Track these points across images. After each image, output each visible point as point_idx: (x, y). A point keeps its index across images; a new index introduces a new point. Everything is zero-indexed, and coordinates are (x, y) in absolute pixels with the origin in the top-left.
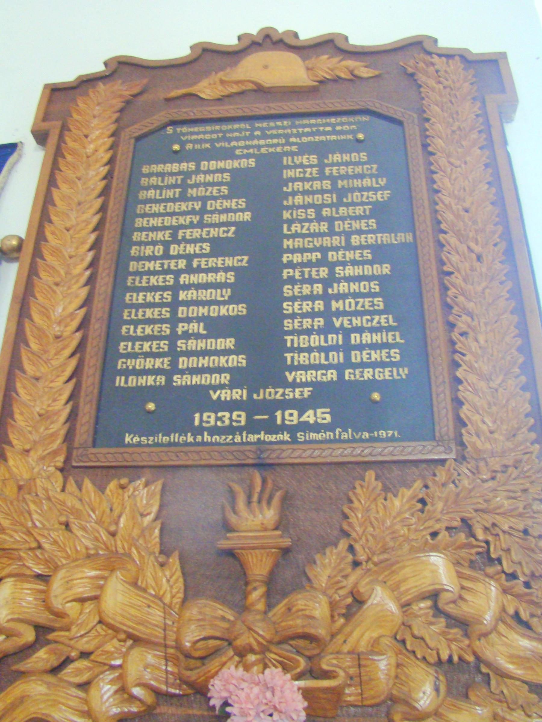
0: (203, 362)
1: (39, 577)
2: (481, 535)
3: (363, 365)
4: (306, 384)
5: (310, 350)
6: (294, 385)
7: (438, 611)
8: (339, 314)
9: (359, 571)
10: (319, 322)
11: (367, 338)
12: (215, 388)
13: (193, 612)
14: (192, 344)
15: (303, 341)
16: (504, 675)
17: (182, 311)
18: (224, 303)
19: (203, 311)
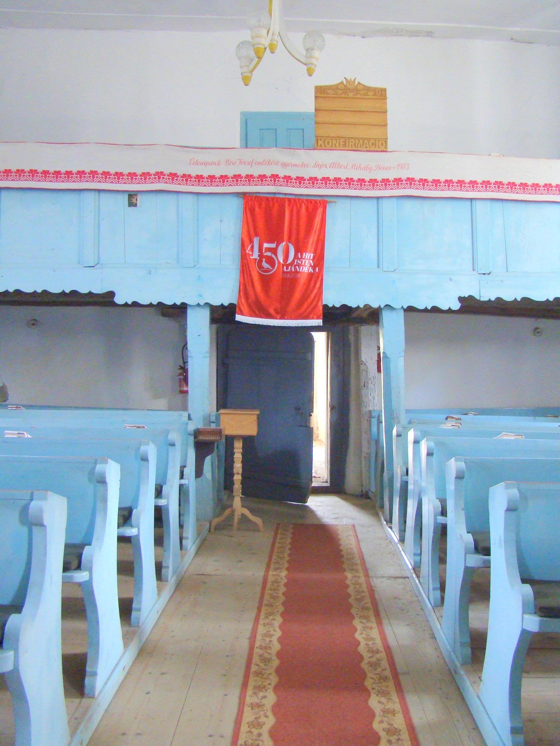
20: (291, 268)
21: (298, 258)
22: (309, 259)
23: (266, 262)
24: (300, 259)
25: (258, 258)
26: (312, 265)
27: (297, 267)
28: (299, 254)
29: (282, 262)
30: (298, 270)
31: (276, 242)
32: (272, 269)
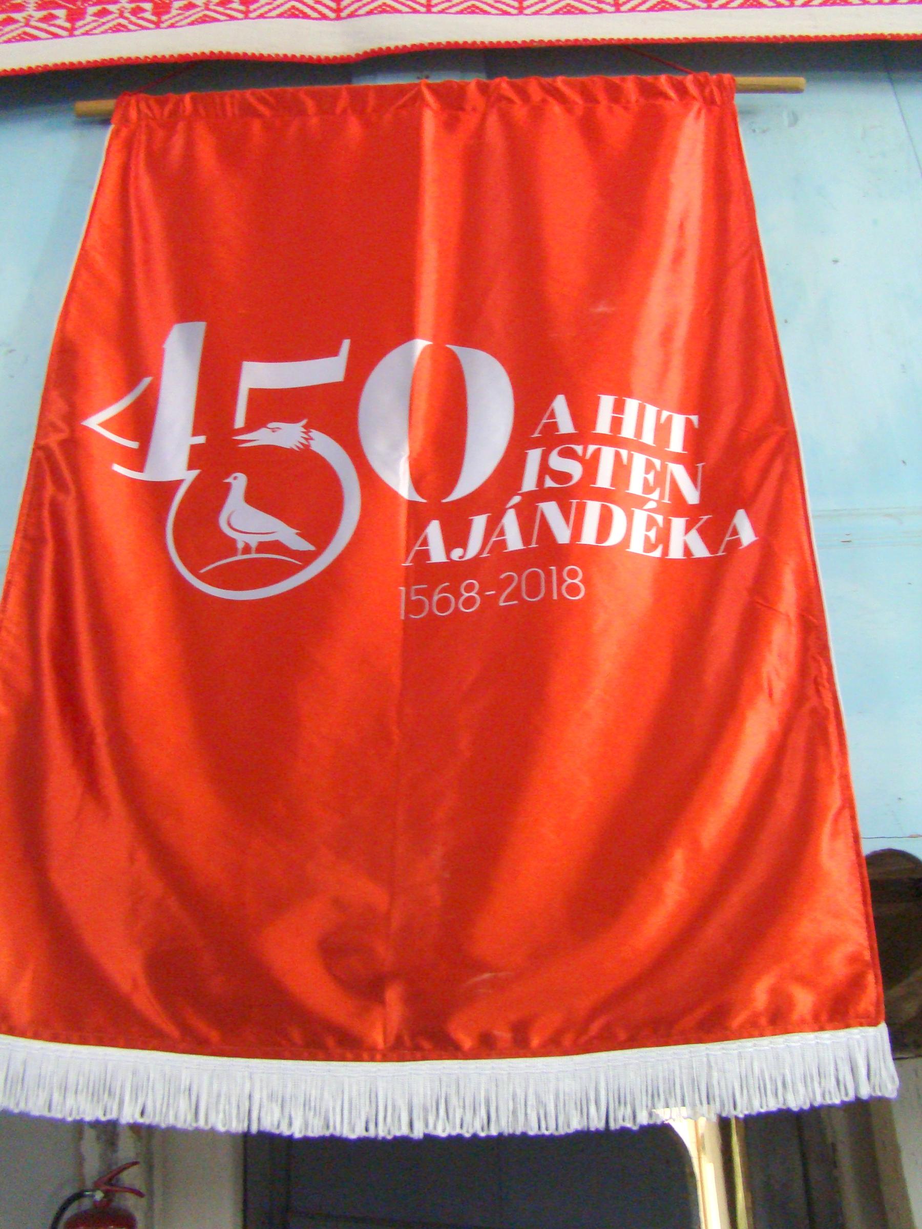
20: (493, 525)
22: (659, 448)
23: (253, 498)
24: (569, 438)
25: (191, 476)
26: (692, 495)
27: (550, 510)
28: (560, 405)
30: (562, 534)
31: (346, 344)
32: (303, 545)
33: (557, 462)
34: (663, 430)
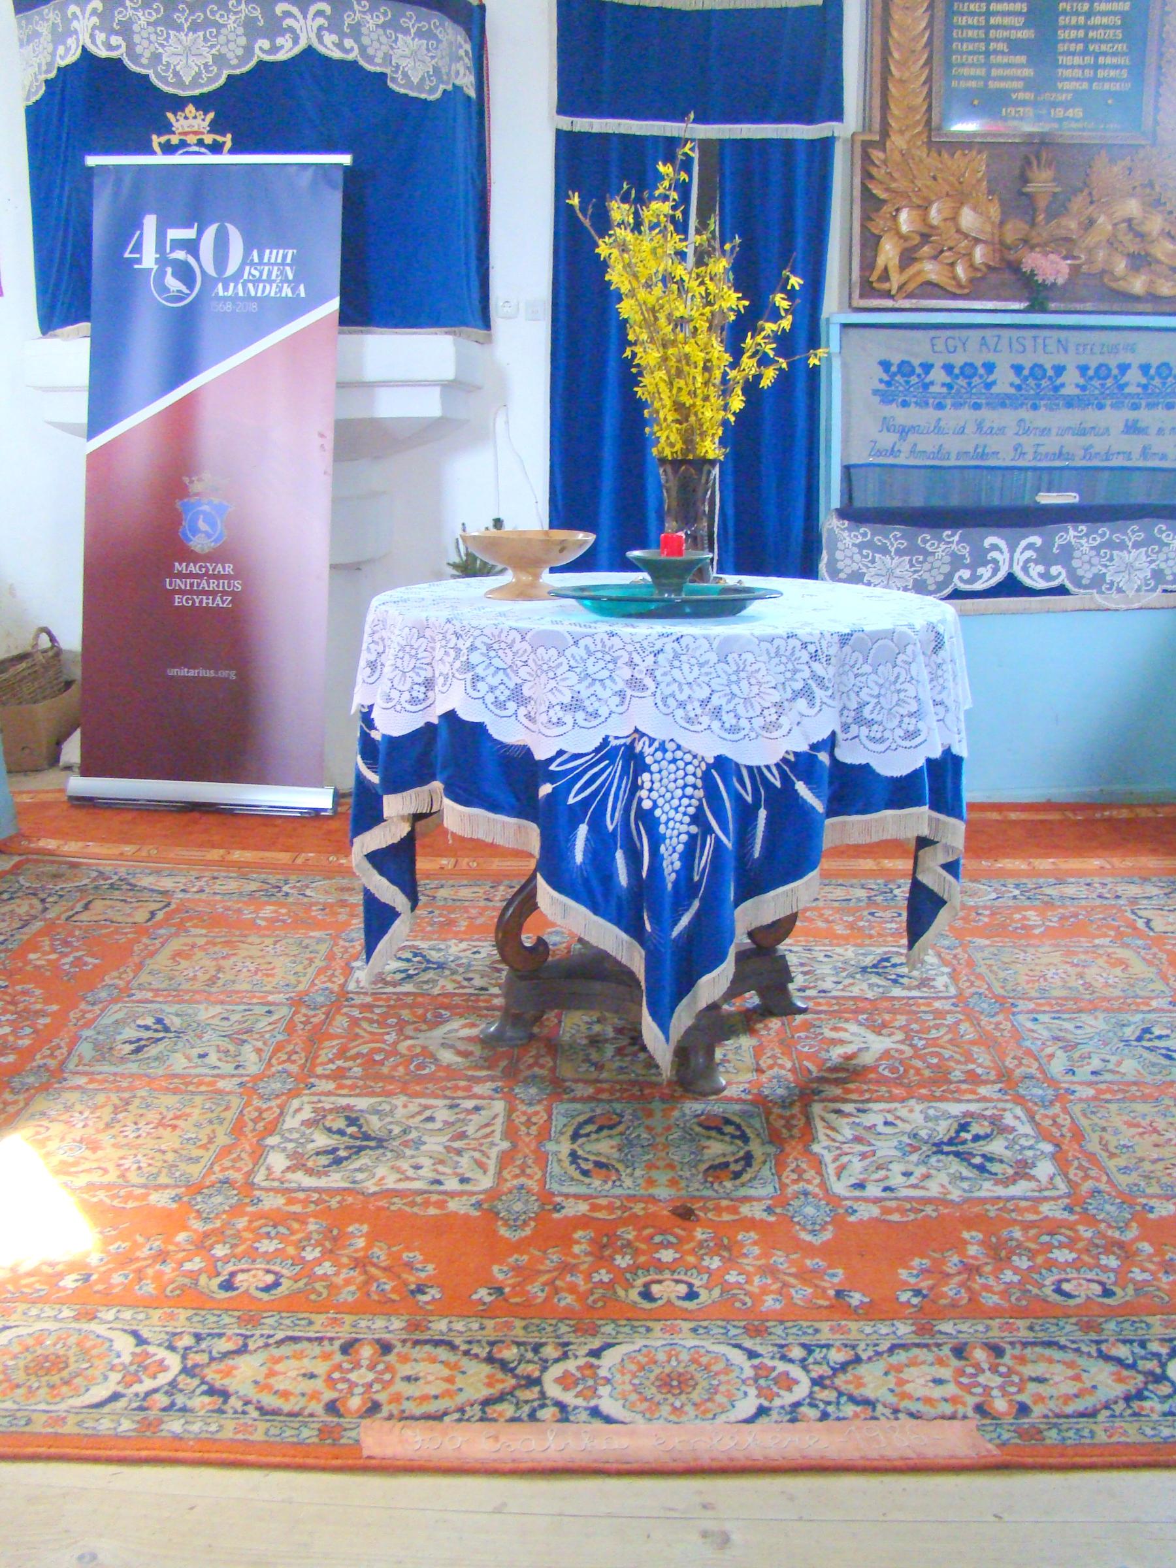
0: (1008, 72)
1: (919, 207)
2: (1157, 189)
3: (1104, 80)
4: (1067, 91)
5: (1072, 67)
6: (1062, 91)
7: (1130, 227)
8: (1094, 41)
9: (1091, 208)
10: (1080, 47)
11: (1108, 60)
12: (1016, 91)
13: (1008, 226)
14: (1000, 59)
15: (1068, 60)
16: (1159, 262)
17: (992, 33)
18: (1019, 28)
19: (1006, 34)
20: (235, 287)
21: (252, 264)
22: (283, 263)
23: (174, 275)
26: (291, 277)
27: (250, 286)
28: (255, 253)
29: (211, 271)
30: (253, 293)
33: (254, 272)
34: (285, 257)
